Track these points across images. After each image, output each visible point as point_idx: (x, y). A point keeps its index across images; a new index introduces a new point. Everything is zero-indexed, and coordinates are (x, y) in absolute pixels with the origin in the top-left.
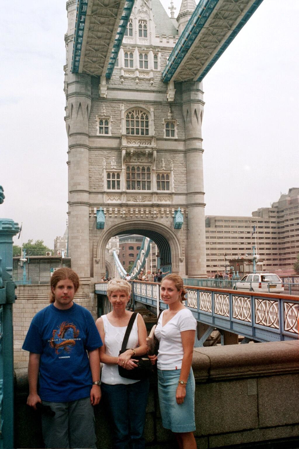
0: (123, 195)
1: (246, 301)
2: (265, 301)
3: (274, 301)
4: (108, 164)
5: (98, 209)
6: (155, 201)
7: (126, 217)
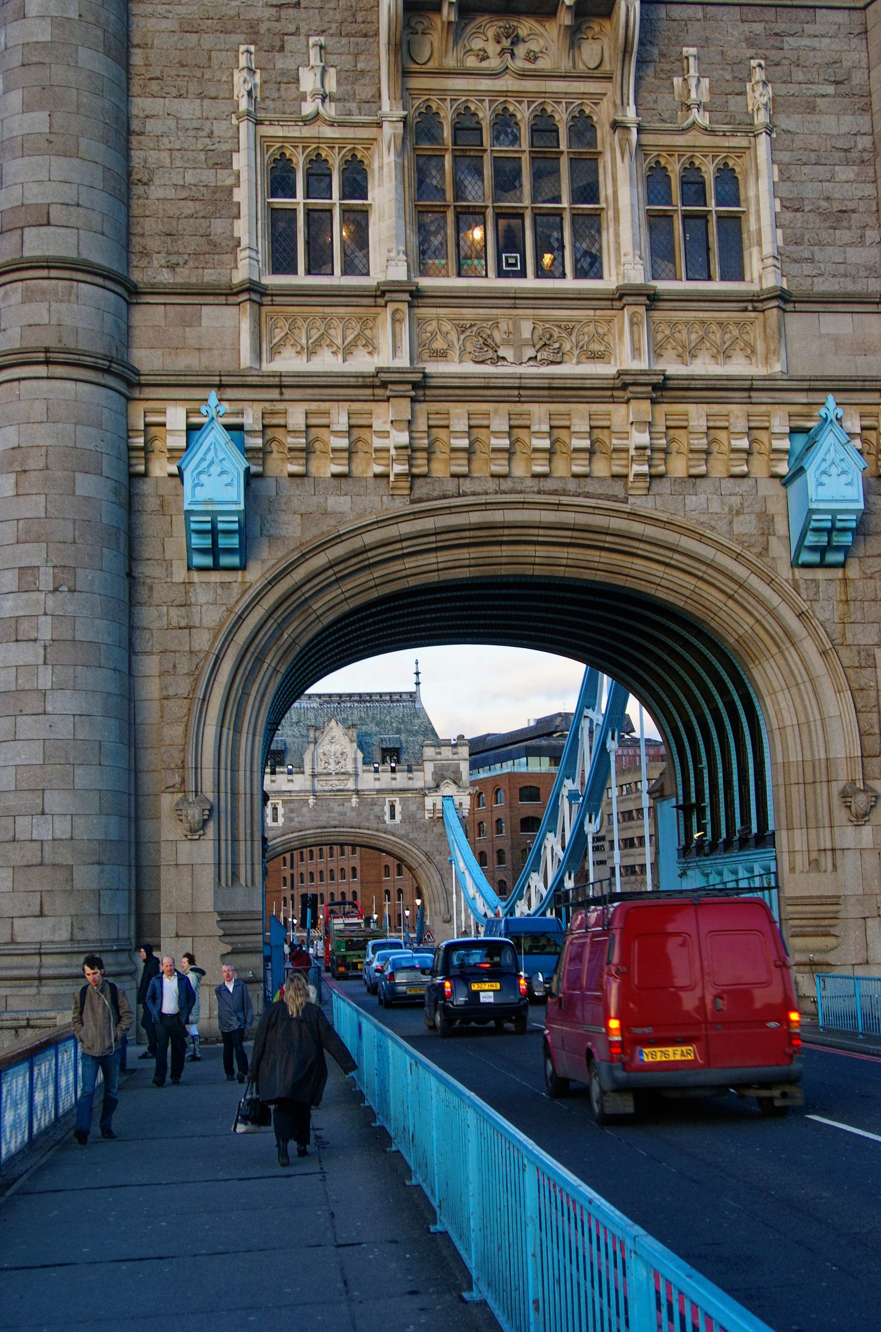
0: (391, 307)
5: (195, 420)
6: (636, 351)
7: (414, 476)
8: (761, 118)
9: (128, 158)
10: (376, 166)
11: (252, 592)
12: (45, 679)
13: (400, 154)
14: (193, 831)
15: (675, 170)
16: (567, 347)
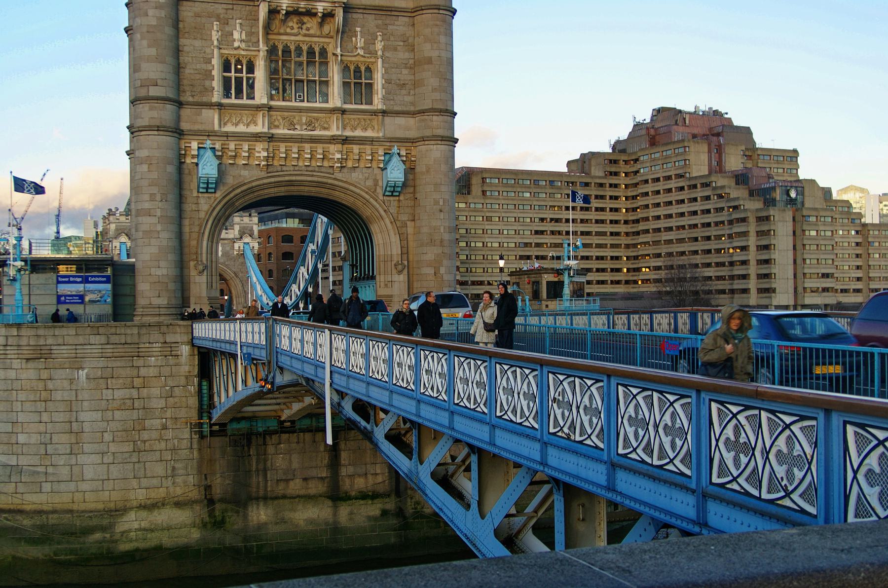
0: (261, 113)
1: (527, 376)
2: (572, 379)
3: (593, 379)
4: (226, 37)
6: (338, 128)
7: (268, 165)
8: (380, 53)
9: (178, 59)
10: (257, 64)
11: (218, 200)
12: (159, 228)
13: (265, 61)
14: (200, 273)
15: (352, 68)
16: (317, 125)
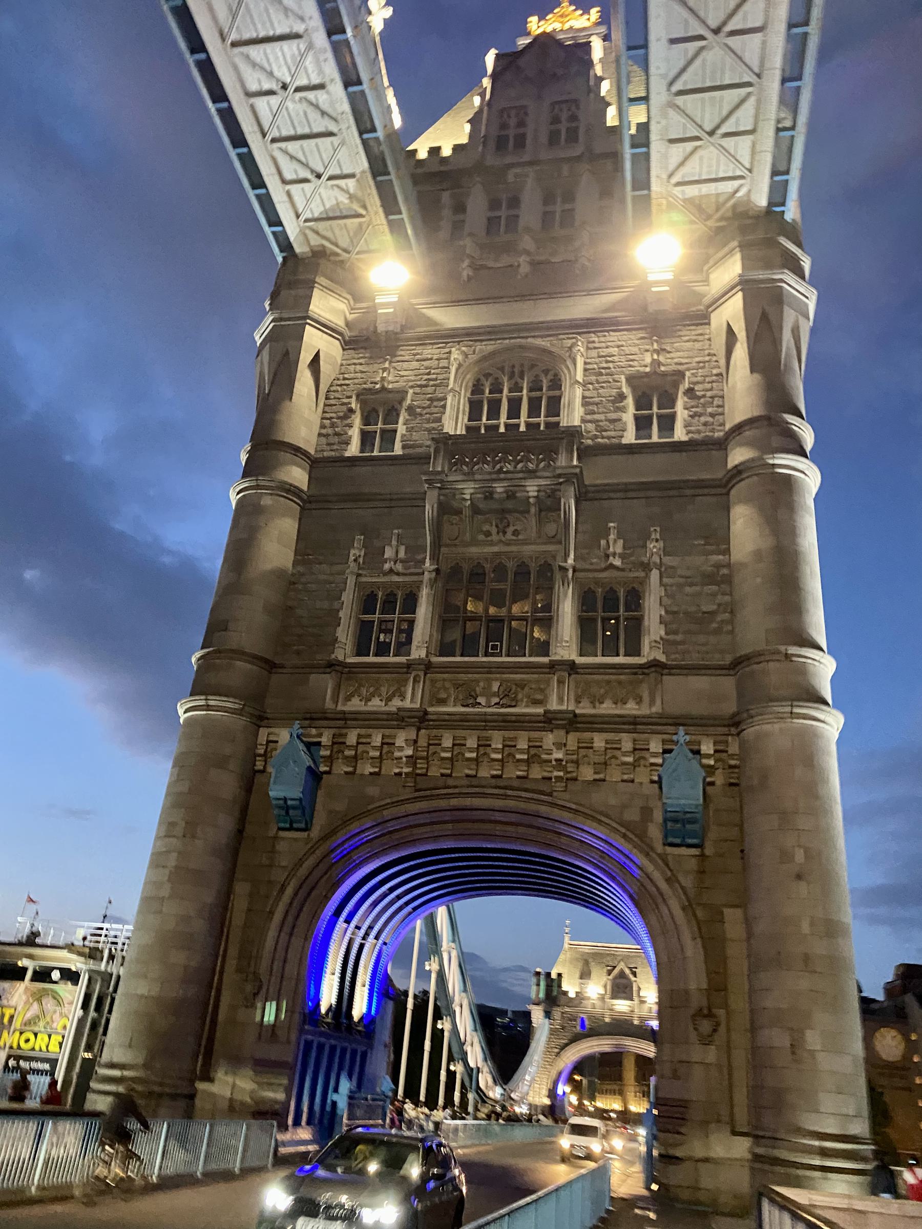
16: (520, 696)
